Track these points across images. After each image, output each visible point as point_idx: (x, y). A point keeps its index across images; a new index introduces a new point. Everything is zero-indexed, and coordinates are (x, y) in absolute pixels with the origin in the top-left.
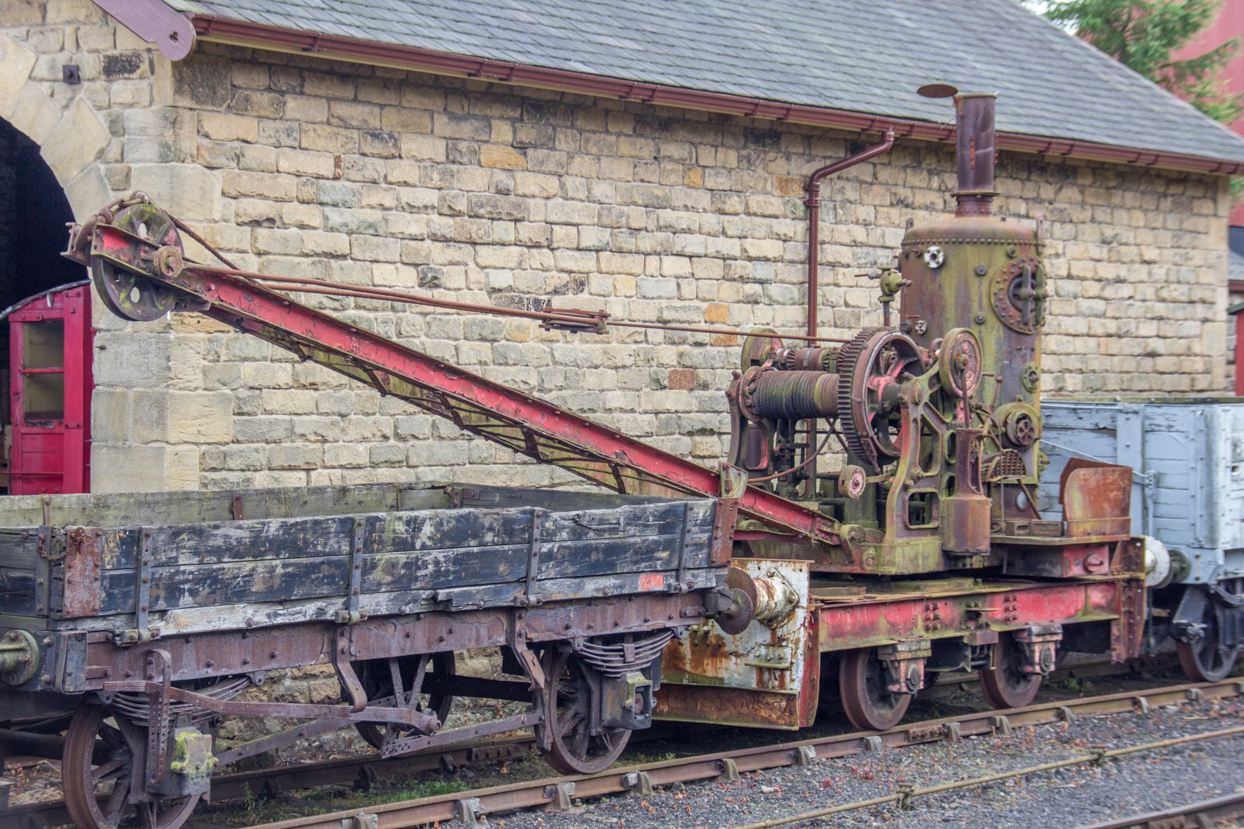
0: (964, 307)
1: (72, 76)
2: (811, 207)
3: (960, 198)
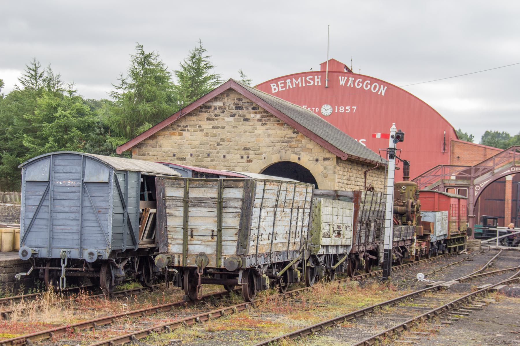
0: (409, 196)
1: (317, 160)
2: (365, 176)
3: (404, 178)
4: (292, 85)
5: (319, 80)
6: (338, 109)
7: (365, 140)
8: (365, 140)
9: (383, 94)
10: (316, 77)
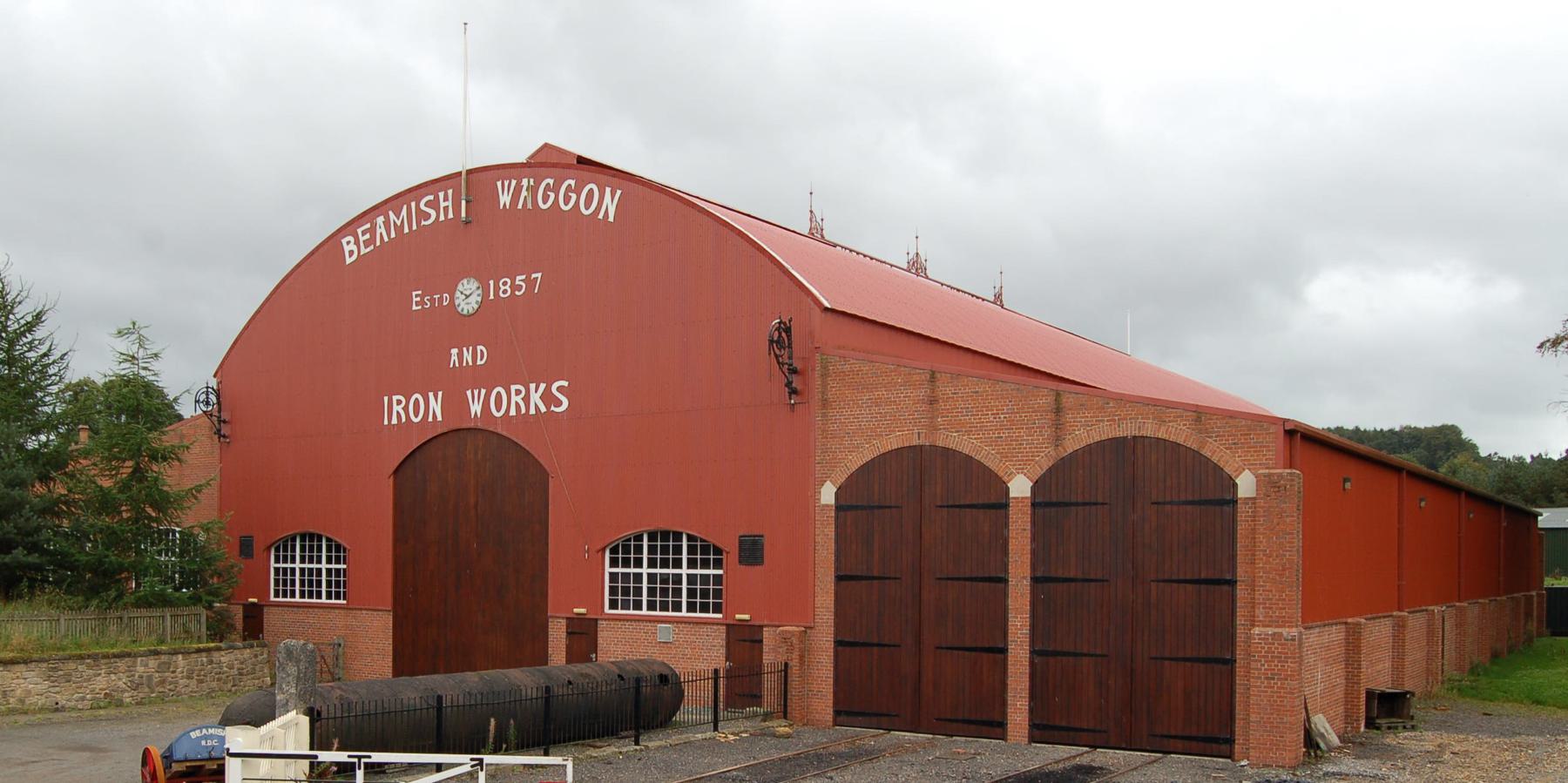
4: (389, 234)
5: (450, 203)
6: (497, 288)
7: (565, 384)
8: (565, 384)
9: (611, 219)
10: (441, 195)
